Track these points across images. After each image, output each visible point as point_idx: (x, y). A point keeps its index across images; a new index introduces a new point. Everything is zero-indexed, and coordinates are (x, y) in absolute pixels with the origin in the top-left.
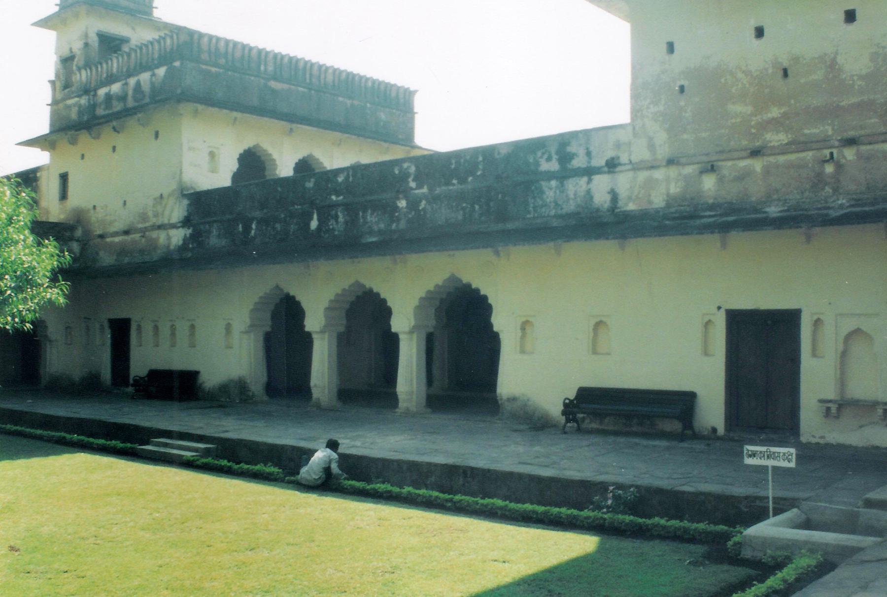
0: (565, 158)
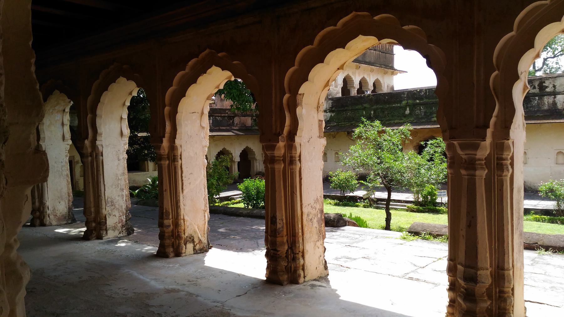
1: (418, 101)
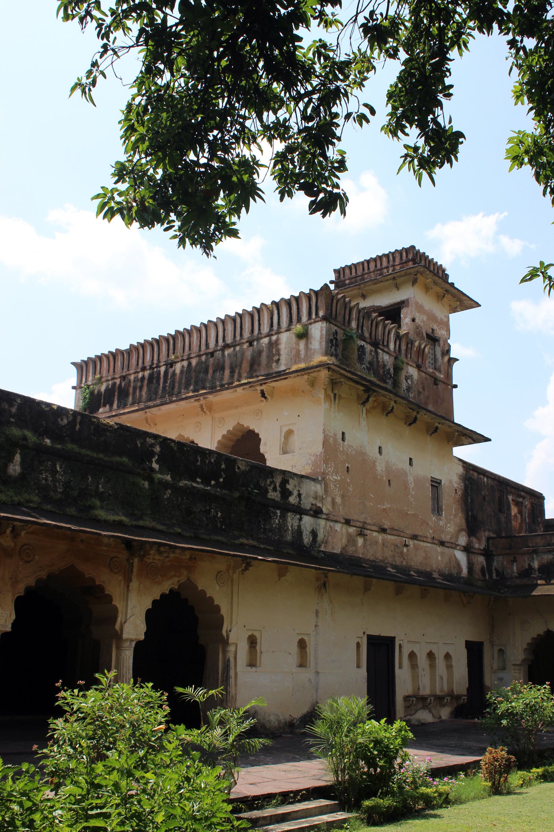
0: (286, 494)
1: (48, 441)
